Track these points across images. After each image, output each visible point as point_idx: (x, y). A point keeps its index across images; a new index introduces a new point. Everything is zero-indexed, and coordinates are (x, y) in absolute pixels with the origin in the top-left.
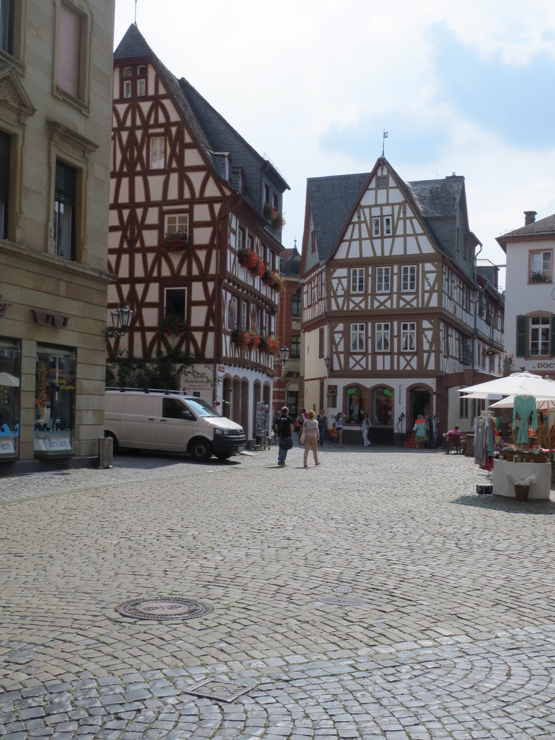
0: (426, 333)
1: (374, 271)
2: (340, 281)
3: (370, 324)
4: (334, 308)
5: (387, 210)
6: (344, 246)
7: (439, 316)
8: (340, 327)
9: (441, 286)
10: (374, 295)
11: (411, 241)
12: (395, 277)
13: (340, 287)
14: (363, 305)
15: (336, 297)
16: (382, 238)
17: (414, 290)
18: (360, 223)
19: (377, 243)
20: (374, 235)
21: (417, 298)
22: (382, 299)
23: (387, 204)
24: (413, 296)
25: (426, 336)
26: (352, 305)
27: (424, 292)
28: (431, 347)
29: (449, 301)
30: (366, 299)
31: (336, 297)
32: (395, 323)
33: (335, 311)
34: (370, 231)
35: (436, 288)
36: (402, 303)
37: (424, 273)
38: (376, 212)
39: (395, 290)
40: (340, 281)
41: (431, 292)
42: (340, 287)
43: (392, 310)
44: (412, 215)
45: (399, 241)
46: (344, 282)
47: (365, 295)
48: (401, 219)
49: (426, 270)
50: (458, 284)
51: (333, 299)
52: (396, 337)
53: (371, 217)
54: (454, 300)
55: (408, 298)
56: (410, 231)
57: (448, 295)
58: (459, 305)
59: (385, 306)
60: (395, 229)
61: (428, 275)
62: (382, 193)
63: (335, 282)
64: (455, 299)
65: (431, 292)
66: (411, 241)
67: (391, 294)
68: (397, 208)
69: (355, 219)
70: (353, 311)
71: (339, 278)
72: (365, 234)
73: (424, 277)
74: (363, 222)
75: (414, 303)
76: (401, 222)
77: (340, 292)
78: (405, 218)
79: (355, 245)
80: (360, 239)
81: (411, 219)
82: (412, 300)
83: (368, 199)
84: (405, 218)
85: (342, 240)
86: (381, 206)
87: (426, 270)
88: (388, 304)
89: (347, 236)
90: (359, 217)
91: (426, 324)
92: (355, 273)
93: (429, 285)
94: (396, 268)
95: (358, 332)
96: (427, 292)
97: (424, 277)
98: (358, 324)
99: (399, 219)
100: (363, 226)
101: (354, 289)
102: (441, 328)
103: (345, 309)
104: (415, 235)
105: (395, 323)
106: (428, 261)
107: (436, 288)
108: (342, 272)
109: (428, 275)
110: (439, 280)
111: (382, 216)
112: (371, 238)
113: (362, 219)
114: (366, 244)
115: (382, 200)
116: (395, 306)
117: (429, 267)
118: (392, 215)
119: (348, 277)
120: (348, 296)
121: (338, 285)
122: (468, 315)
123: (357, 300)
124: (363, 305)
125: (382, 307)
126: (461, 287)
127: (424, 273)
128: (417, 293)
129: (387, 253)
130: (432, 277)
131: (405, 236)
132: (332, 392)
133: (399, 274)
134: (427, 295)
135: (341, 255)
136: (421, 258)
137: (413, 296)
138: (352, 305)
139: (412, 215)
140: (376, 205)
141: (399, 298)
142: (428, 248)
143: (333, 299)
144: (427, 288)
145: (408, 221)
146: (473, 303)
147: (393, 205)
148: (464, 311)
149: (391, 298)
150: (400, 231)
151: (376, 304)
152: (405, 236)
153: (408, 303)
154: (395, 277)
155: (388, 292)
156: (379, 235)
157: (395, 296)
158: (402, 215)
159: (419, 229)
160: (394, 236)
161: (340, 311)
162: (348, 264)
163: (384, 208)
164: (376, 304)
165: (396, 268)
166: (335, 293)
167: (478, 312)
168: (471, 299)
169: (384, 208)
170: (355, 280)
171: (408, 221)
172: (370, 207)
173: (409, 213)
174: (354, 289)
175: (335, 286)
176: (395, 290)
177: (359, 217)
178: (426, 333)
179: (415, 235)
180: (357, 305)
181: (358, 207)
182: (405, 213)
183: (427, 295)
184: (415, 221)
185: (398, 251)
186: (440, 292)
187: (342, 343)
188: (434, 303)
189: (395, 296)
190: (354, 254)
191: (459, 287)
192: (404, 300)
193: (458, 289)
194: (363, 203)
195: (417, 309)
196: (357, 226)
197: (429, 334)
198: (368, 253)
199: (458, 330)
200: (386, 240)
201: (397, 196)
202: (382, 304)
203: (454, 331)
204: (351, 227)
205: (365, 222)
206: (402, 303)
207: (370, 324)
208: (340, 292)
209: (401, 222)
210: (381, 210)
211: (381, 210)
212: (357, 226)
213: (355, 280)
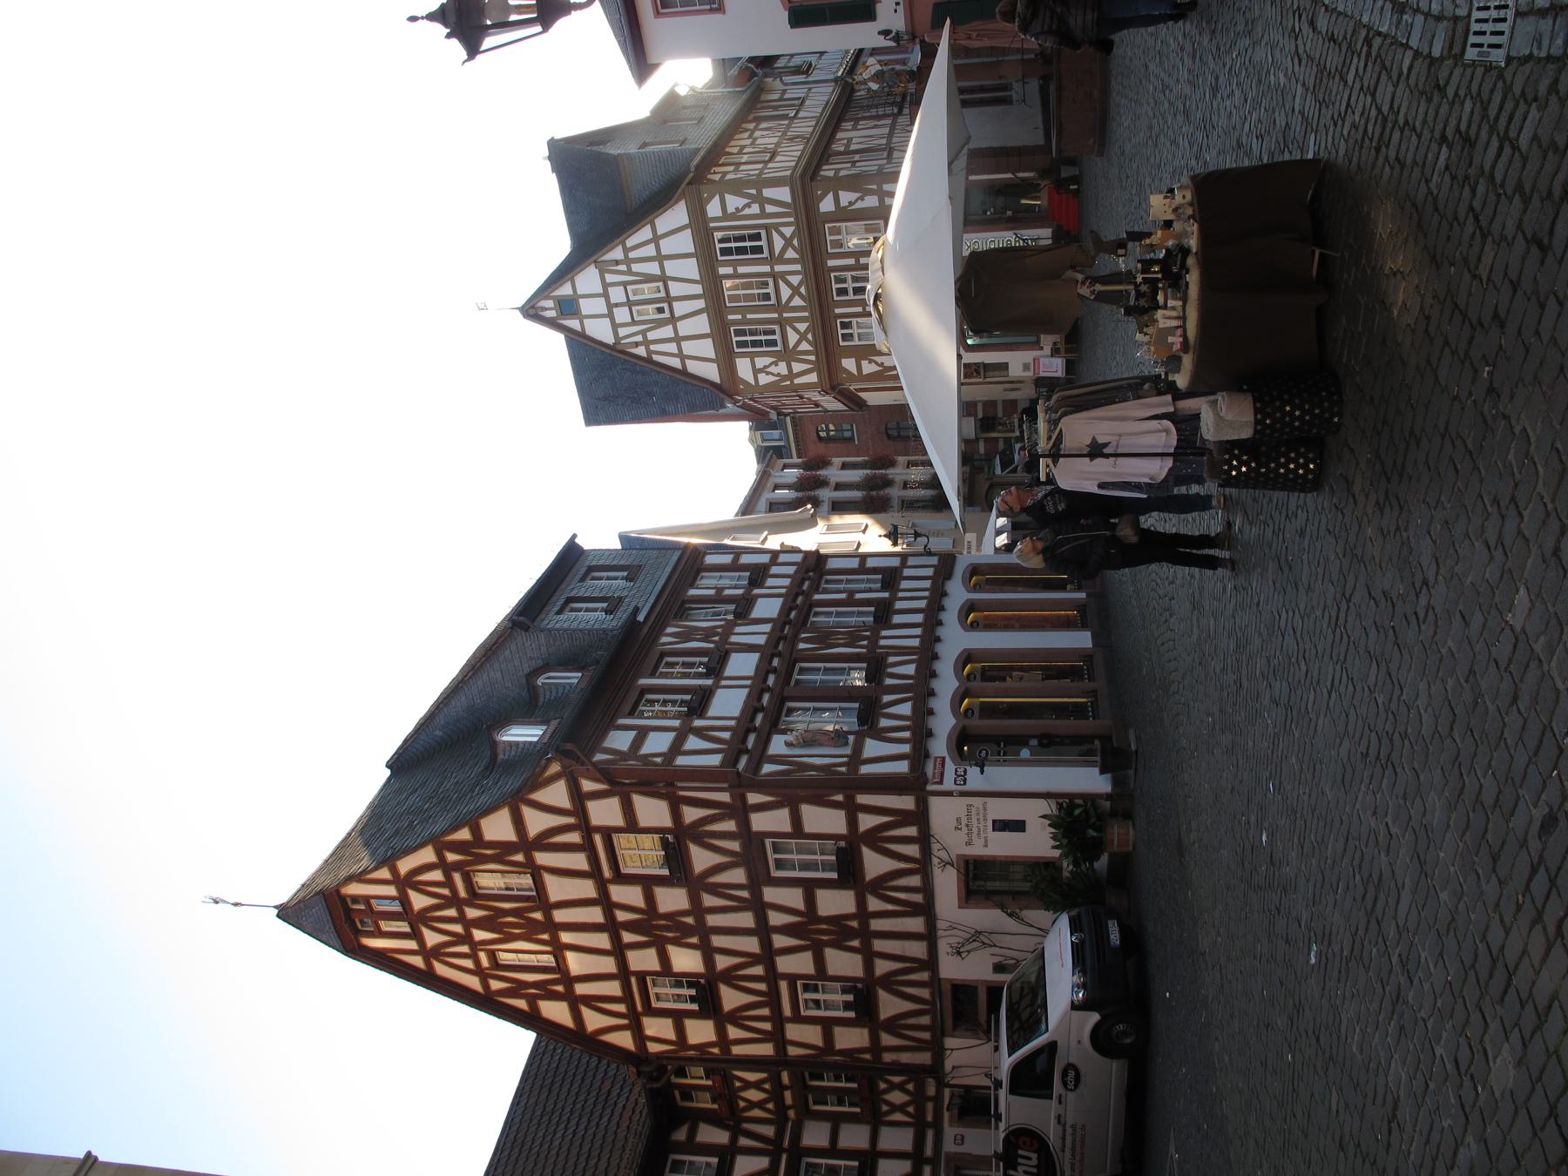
0: (844, 203)
1: (735, 310)
2: (761, 370)
3: (838, 311)
4: (813, 378)
5: (617, 295)
6: (694, 367)
7: (808, 179)
8: (849, 364)
9: (748, 183)
10: (780, 307)
11: (667, 246)
12: (741, 270)
13: (773, 369)
14: (802, 327)
15: (791, 375)
16: (669, 299)
17: (763, 233)
18: (646, 343)
19: (680, 308)
20: (667, 315)
21: (776, 227)
22: (786, 293)
23: (606, 295)
24: (775, 234)
25: (851, 203)
26: (805, 346)
27: (763, 214)
28: (871, 193)
29: (778, 158)
30: (791, 321)
31: (791, 375)
32: (831, 263)
33: (819, 377)
34: (659, 324)
35: (753, 192)
36: (791, 254)
37: (726, 216)
38: (622, 315)
39: (767, 269)
40: (761, 370)
41: (762, 201)
42: (773, 369)
43: (805, 273)
44: (620, 248)
45: (672, 268)
46: (761, 362)
47: (782, 323)
48: (629, 268)
49: (720, 214)
50: (746, 135)
51: (797, 381)
52: (857, 261)
53: (634, 322)
54: (777, 145)
55: (778, 243)
56: (650, 251)
57: (766, 163)
58: (789, 126)
59: (800, 285)
60: (649, 278)
61: (731, 209)
62: (586, 306)
63: (764, 379)
64: (775, 140)
65: (762, 201)
66: (667, 246)
67: (774, 275)
68: (610, 278)
69: (641, 351)
70: (814, 344)
71: (756, 372)
72: (667, 332)
73: (733, 217)
74: (645, 337)
75: (788, 231)
76: (636, 268)
77: (782, 368)
78: (628, 261)
79: (689, 348)
80: (678, 339)
81: (626, 251)
82: (782, 235)
83: (600, 331)
84: (628, 261)
85: (684, 372)
86: (610, 306)
87: (720, 214)
88: (795, 280)
89: (675, 363)
90: (637, 344)
91: (827, 205)
92: (741, 344)
93: (748, 205)
94: (722, 271)
95: (855, 331)
96: (762, 209)
97: (733, 217)
98: (840, 332)
99: (630, 272)
100: (651, 336)
101: (774, 343)
102: (831, 174)
103: (813, 358)
104: (656, 239)
105: (831, 263)
106: (703, 212)
107: (753, 192)
108: (744, 368)
109: (731, 209)
110: (737, 188)
111: (630, 304)
112: (673, 320)
113: (639, 338)
114: (685, 328)
115: (599, 306)
116: (798, 267)
117: (713, 209)
118: (625, 284)
119: (752, 356)
120: (788, 355)
121: (768, 373)
122: (807, 102)
123: (793, 338)
124: (802, 327)
125: (803, 290)
126: (752, 126)
127: (726, 216)
128: (767, 227)
129: (698, 289)
130: (733, 202)
131: (660, 258)
132: (978, 373)
133: (734, 264)
134: (770, 209)
135: (711, 372)
136: (700, 226)
137: (775, 234)
138: (805, 346)
139: (620, 248)
140: (610, 315)
141: (781, 260)
142: (676, 215)
143: (797, 381)
144: (755, 209)
145: (632, 255)
146: (784, 91)
147: (605, 285)
148: (801, 114)
149: (783, 275)
150: (653, 268)
151: (797, 301)
152: (660, 258)
153: (788, 243)
154: (741, 270)
155: (771, 281)
156: (665, 305)
157: (778, 268)
158: (623, 267)
159: (645, 233)
160: (664, 279)
161: (816, 367)
162: (726, 358)
163: (613, 301)
164: (797, 301)
165: (722, 271)
166: (784, 378)
167: (801, 78)
168: (776, 96)
169: (613, 301)
170: (755, 344)
171: (632, 255)
172: (615, 326)
173: (617, 253)
174: (774, 343)
175: (771, 379)
176: (767, 269)
177: (637, 344)
178: (844, 203)
179: (656, 239)
180: (803, 337)
181: (619, 347)
182: (617, 263)
183: (770, 209)
184: (630, 242)
185: (690, 268)
186: (762, 182)
187: (879, 359)
188: (784, 194)
189: (778, 268)
190: (707, 348)
191: (753, 131)
192: (784, 250)
193: (757, 134)
194: (610, 340)
195: (797, 224)
196: (652, 347)
197: (846, 197)
198: (702, 324)
199: (837, 128)
200: (673, 293)
201: (588, 280)
202: (795, 291)
203: (839, 135)
204: (656, 358)
205: (644, 333)
206: (791, 254)
207: (838, 311)
208: (782, 368)
209: (636, 268)
210: (617, 305)
211: (617, 305)
212: (652, 347)
213: (755, 344)
